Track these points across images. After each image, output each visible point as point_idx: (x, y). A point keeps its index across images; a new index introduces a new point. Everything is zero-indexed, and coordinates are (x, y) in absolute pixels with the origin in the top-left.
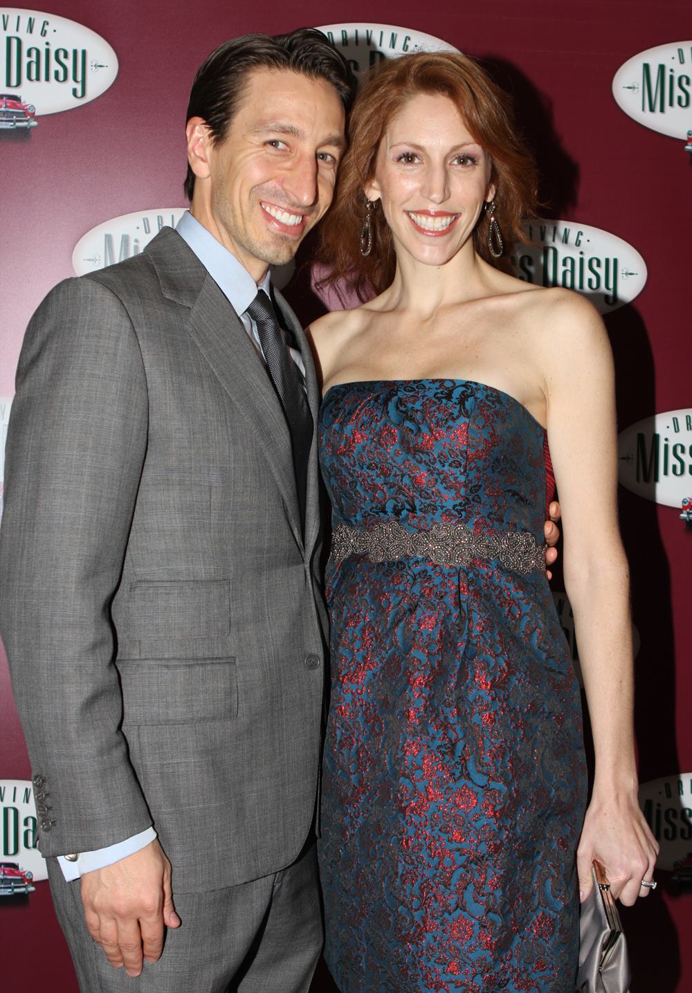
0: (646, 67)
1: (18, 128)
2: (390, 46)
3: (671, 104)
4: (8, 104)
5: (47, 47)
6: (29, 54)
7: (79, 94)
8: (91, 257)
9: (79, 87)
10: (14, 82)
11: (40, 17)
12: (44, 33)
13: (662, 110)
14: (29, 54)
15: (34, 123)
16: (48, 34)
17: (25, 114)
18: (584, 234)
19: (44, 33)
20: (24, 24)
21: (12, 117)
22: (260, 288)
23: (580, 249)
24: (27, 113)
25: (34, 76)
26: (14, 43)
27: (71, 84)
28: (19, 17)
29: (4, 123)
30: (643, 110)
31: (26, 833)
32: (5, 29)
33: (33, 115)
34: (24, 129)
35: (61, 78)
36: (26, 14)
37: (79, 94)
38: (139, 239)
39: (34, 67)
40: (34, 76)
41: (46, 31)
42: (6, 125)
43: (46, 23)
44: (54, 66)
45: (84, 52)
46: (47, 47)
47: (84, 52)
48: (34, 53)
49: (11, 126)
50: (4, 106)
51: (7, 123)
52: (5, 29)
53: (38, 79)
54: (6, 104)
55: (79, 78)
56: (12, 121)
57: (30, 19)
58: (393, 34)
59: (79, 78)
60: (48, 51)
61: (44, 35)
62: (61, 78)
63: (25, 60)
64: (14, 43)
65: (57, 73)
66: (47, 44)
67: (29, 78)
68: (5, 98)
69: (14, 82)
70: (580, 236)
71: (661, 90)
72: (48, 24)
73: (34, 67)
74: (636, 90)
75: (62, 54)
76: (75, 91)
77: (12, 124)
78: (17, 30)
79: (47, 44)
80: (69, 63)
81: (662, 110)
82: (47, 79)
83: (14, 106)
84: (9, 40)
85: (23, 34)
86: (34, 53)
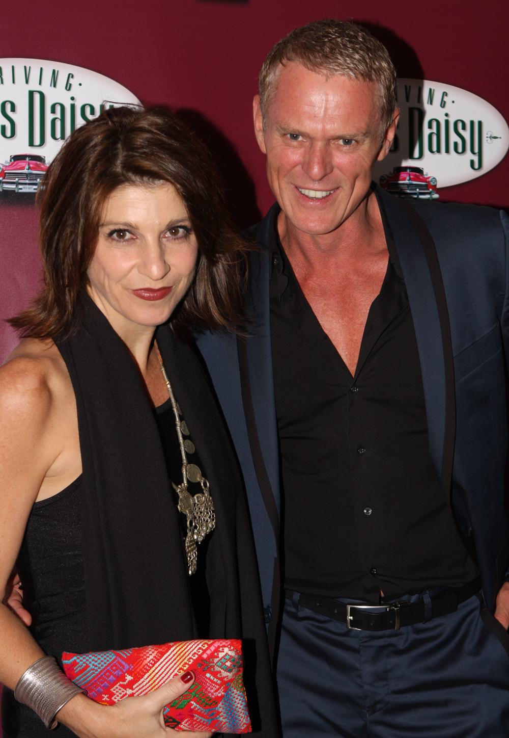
4: (31, 166)
5: (72, 102)
6: (53, 111)
10: (37, 141)
11: (64, 69)
12: (68, 87)
14: (53, 111)
16: (73, 88)
19: (68, 87)
21: (36, 180)
26: (37, 97)
29: (27, 186)
32: (27, 82)
36: (49, 66)
39: (58, 124)
41: (71, 85)
42: (29, 188)
43: (71, 76)
46: (72, 102)
48: (58, 109)
49: (35, 189)
50: (27, 167)
51: (30, 186)
52: (27, 82)
54: (29, 164)
56: (35, 184)
57: (54, 71)
61: (69, 90)
63: (49, 117)
64: (37, 97)
66: (73, 99)
67: (53, 136)
68: (27, 159)
69: (37, 141)
72: (72, 77)
73: (58, 124)
77: (36, 187)
79: (73, 99)
83: (37, 167)
84: (31, 94)
85: (46, 88)
86: (58, 109)
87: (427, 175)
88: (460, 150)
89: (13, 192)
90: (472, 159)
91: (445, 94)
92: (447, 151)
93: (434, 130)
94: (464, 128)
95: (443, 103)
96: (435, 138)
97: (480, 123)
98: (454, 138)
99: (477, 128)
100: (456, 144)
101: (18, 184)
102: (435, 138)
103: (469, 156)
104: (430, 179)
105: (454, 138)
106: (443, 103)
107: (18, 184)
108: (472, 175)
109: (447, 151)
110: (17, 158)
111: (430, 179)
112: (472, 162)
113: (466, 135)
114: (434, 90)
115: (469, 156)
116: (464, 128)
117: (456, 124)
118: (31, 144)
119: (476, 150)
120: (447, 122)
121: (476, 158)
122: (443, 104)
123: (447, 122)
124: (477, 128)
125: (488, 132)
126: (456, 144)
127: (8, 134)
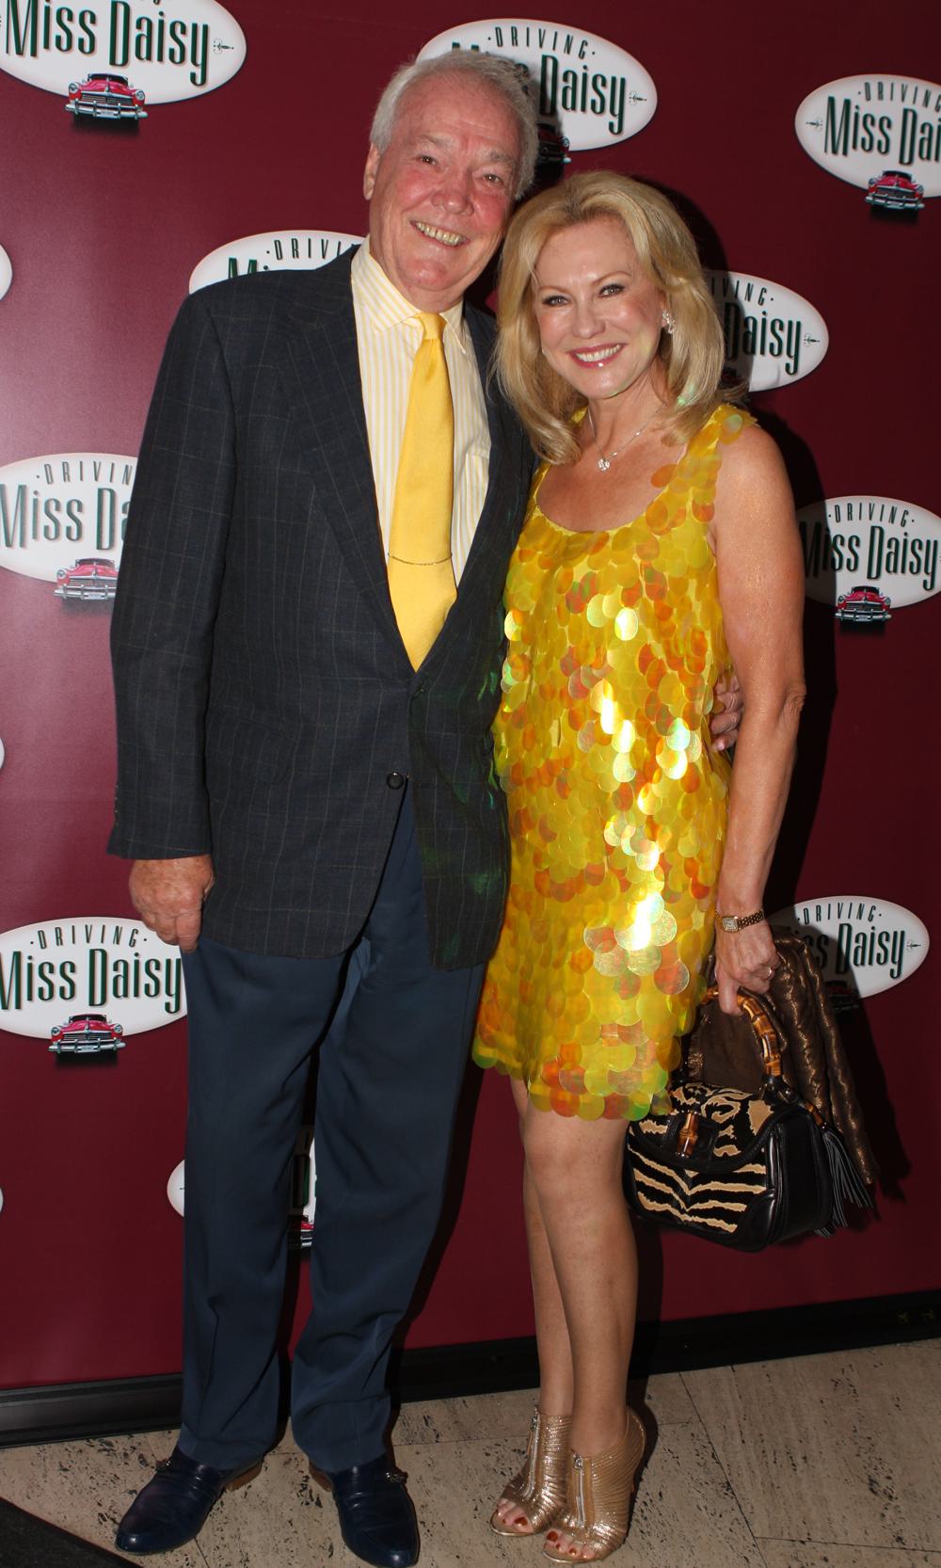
0: (831, 101)
1: (124, 118)
3: (855, 147)
7: (199, 80)
9: (198, 71)
10: (119, 60)
13: (845, 153)
15: (143, 114)
17: (133, 101)
24: (134, 100)
25: (144, 54)
27: (189, 67)
31: (116, 979)
33: (141, 103)
34: (131, 119)
35: (177, 59)
37: (199, 80)
40: (144, 54)
44: (169, 43)
45: (206, 28)
47: (206, 28)
48: (145, 24)
53: (149, 58)
55: (199, 61)
59: (199, 61)
60: (161, 23)
62: (177, 59)
63: (134, 33)
65: (172, 51)
69: (119, 60)
71: (845, 129)
73: (144, 41)
75: (178, 28)
76: (193, 77)
80: (187, 41)
81: (845, 153)
82: (160, 59)
83: (118, 90)
89: (89, 116)
92: (583, 109)
94: (604, 84)
97: (623, 81)
98: (591, 95)
99: (619, 86)
100: (593, 102)
101: (95, 107)
105: (591, 95)
107: (95, 107)
108: (611, 139)
109: (583, 109)
110: (96, 77)
112: (611, 125)
113: (607, 93)
116: (604, 84)
117: (595, 78)
118: (113, 62)
121: (616, 121)
122: (582, 55)
123: (585, 76)
124: (619, 86)
126: (593, 102)
127: (87, 48)
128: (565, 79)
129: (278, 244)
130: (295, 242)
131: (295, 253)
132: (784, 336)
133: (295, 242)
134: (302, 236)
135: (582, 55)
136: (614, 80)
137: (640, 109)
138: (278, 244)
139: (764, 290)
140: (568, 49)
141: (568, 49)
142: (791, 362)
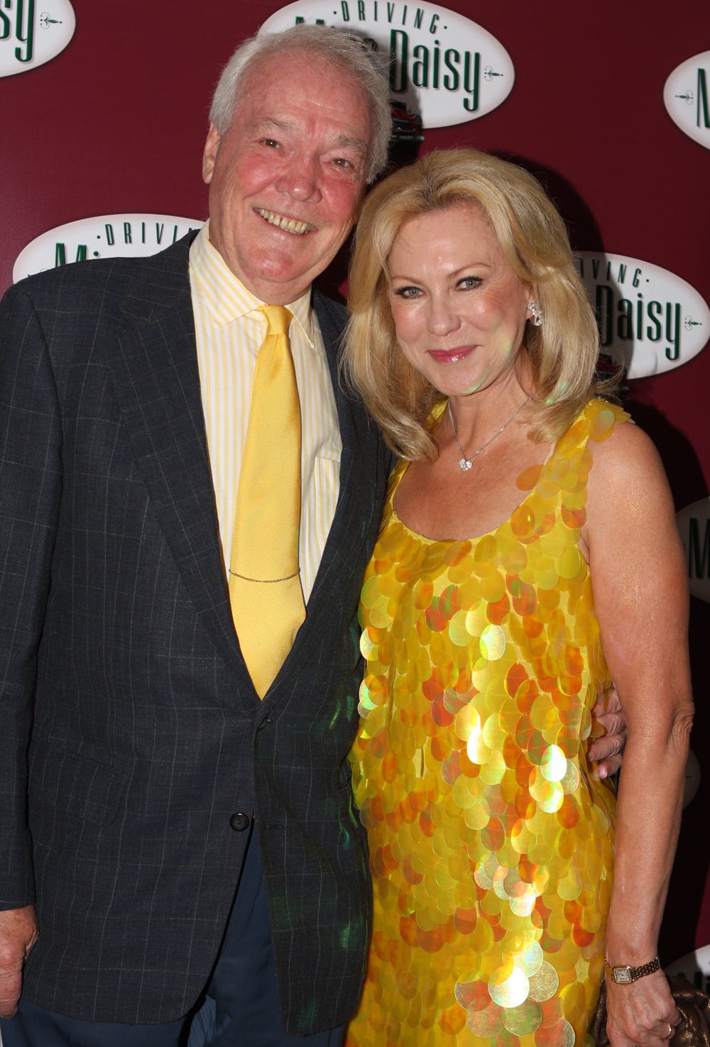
2: (415, 26)
8: (693, 326)
18: (642, 273)
20: (411, 16)
22: (607, 351)
23: (638, 290)
28: (406, 7)
30: (698, 125)
38: (642, 293)
58: (419, 10)
70: (638, 275)
74: (690, 100)
78: (404, 23)
87: (410, 111)
88: (452, 85)
90: (466, 97)
91: (436, 17)
92: (436, 85)
93: (421, 59)
94: (457, 60)
95: (433, 27)
96: (421, 68)
98: (444, 70)
100: (446, 78)
102: (421, 68)
103: (462, 94)
104: (414, 117)
105: (444, 70)
106: (433, 27)
108: (468, 116)
109: (436, 85)
111: (414, 117)
112: (466, 102)
114: (423, 11)
115: (462, 94)
117: (448, 53)
119: (472, 87)
120: (437, 51)
121: (471, 97)
122: (433, 29)
123: (437, 51)
125: (487, 67)
126: (446, 78)
128: (416, 55)
129: (109, 228)
130: (127, 227)
131: (128, 238)
132: (662, 319)
133: (127, 227)
134: (136, 220)
135: (433, 29)
136: (468, 54)
137: (496, 88)
138: (109, 228)
139: (638, 271)
140: (418, 23)
141: (418, 23)
142: (672, 347)
